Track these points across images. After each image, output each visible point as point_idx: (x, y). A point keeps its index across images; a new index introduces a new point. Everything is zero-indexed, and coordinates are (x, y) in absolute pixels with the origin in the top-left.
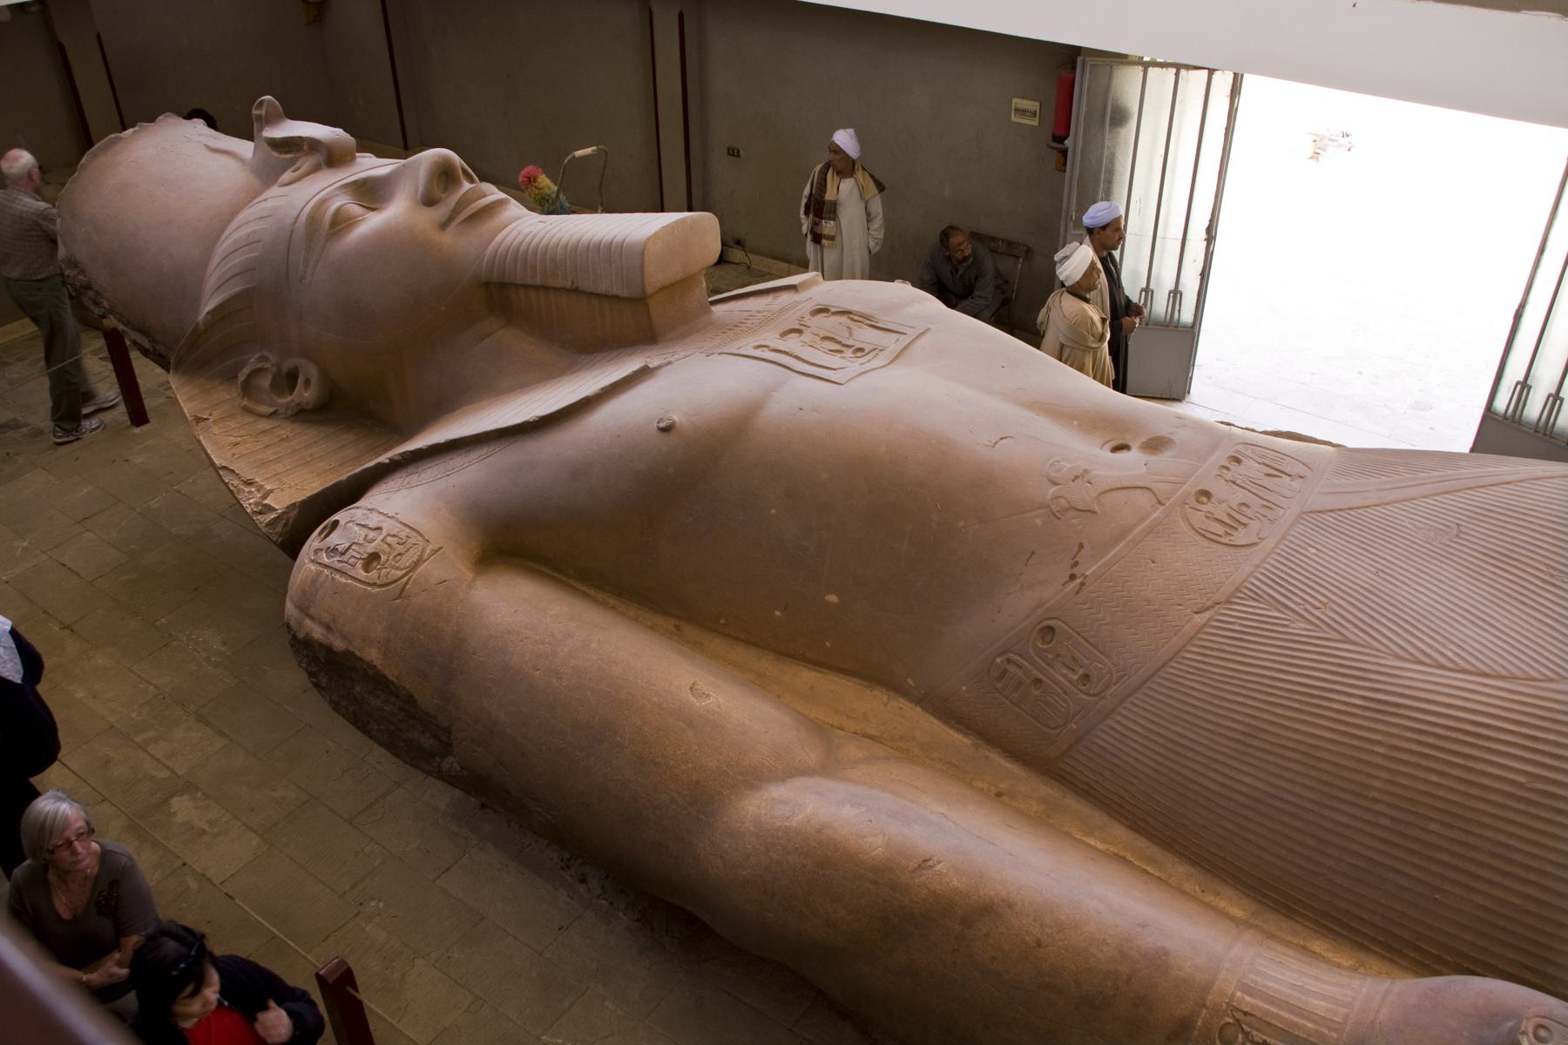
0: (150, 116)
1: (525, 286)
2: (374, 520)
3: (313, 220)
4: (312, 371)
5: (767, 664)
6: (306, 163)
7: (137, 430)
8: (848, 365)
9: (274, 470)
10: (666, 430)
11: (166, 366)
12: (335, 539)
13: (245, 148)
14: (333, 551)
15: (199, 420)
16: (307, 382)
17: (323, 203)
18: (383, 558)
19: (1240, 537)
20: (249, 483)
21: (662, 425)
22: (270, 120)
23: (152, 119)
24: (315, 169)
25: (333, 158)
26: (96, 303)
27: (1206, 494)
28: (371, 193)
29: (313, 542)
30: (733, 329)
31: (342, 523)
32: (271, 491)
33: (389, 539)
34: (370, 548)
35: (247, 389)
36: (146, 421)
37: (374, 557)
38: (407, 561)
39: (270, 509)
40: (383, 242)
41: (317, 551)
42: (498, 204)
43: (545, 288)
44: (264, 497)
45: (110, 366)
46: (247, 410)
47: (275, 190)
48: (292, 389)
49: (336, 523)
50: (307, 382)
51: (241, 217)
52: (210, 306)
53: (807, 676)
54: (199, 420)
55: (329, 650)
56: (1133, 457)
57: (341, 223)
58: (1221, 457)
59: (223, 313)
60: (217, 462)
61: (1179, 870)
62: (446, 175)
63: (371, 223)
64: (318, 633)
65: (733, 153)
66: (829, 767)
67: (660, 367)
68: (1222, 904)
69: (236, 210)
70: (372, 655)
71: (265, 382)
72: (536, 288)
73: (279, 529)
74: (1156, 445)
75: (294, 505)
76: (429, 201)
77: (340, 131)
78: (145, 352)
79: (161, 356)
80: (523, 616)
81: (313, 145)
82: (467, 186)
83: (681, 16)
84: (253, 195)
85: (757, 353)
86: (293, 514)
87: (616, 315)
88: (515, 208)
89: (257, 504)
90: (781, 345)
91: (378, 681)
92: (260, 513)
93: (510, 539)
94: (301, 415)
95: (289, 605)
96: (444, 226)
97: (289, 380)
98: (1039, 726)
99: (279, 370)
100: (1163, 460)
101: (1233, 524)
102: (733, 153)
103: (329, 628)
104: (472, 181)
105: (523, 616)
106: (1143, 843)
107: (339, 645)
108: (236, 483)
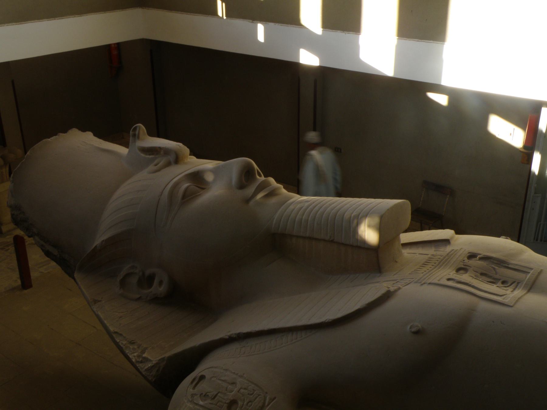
1: (298, 237)
6: (163, 161)
12: (203, 386)
13: (123, 150)
14: (204, 396)
16: (161, 283)
18: (240, 403)
20: (132, 343)
21: (414, 330)
23: (65, 131)
24: (168, 164)
31: (207, 377)
32: (146, 348)
33: (242, 391)
34: (230, 396)
35: (123, 283)
36: (30, 286)
39: (146, 360)
41: (193, 395)
43: (310, 238)
44: (143, 352)
48: (150, 285)
50: (161, 283)
60: (112, 329)
62: (247, 175)
67: (395, 291)
71: (134, 280)
72: (304, 238)
75: (163, 359)
77: (181, 144)
81: (167, 151)
85: (450, 283)
89: (139, 356)
92: (141, 362)
94: (156, 300)
96: (247, 201)
97: (148, 281)
104: (260, 176)
108: (124, 342)
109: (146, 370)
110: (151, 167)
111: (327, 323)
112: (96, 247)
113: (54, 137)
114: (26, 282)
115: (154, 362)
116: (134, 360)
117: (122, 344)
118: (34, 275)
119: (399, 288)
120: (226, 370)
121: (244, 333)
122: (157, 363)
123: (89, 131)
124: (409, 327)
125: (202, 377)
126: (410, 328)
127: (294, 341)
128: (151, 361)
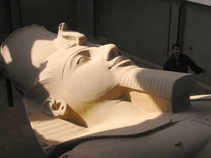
0: (30, 24)
4: (64, 104)
7: (10, 108)
10: (178, 145)
15: (30, 113)
16: (63, 108)
21: (176, 143)
26: (7, 74)
31: (69, 156)
45: (6, 88)
49: (67, 156)
50: (63, 108)
54: (30, 113)
65: (191, 48)
73: (49, 152)
75: (54, 145)
79: (21, 91)
83: (180, 8)
86: (53, 148)
92: (44, 146)
96: (110, 68)
99: (55, 102)
102: (191, 48)
109: (45, 150)
111: (133, 135)
112: (34, 85)
113: (25, 28)
115: (50, 147)
116: (41, 145)
117: (37, 136)
119: (179, 121)
120: (79, 154)
121: (93, 137)
122: (51, 148)
123: (43, 25)
124: (174, 142)
125: (67, 156)
126: (175, 142)
127: (115, 143)
128: (49, 146)
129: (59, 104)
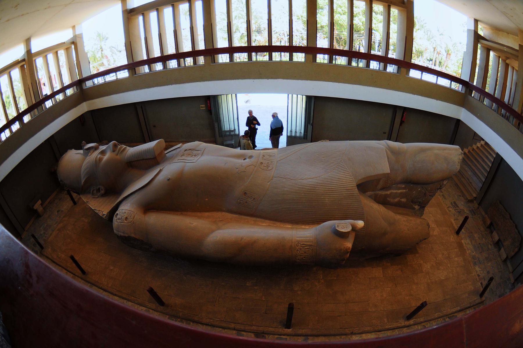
2: (124, 211)
3: (96, 160)
4: (102, 187)
5: (199, 214)
6: (92, 151)
8: (196, 158)
9: (101, 207)
11: (79, 194)
12: (118, 216)
13: (81, 151)
14: (119, 219)
17: (97, 157)
19: (269, 168)
22: (84, 146)
24: (94, 152)
25: (96, 148)
27: (262, 163)
28: (103, 153)
29: (115, 218)
30: (172, 158)
34: (125, 216)
35: (93, 194)
37: (126, 218)
38: (132, 217)
40: (109, 161)
42: (125, 149)
43: (138, 160)
46: (94, 198)
47: (88, 157)
49: (117, 214)
51: (83, 165)
52: (83, 181)
53: (207, 214)
55: (125, 237)
56: (247, 160)
57: (101, 159)
58: (261, 156)
59: (86, 182)
61: (278, 224)
62: (115, 146)
63: (106, 158)
64: (122, 234)
66: (219, 228)
68: (287, 226)
69: (82, 164)
70: (133, 235)
71: (95, 192)
74: (251, 157)
76: (114, 151)
78: (74, 192)
80: (161, 221)
82: (119, 147)
84: (84, 160)
87: (151, 161)
88: (128, 148)
90: (181, 158)
91: (135, 239)
93: (149, 207)
94: (103, 196)
95: (115, 231)
96: (117, 155)
97: (99, 190)
98: (249, 209)
100: (252, 160)
101: (268, 167)
103: (123, 233)
105: (155, 220)
106: (272, 222)
107: (127, 235)
110: (90, 154)
114: (75, 203)
118: (76, 200)
129: (99, 189)
